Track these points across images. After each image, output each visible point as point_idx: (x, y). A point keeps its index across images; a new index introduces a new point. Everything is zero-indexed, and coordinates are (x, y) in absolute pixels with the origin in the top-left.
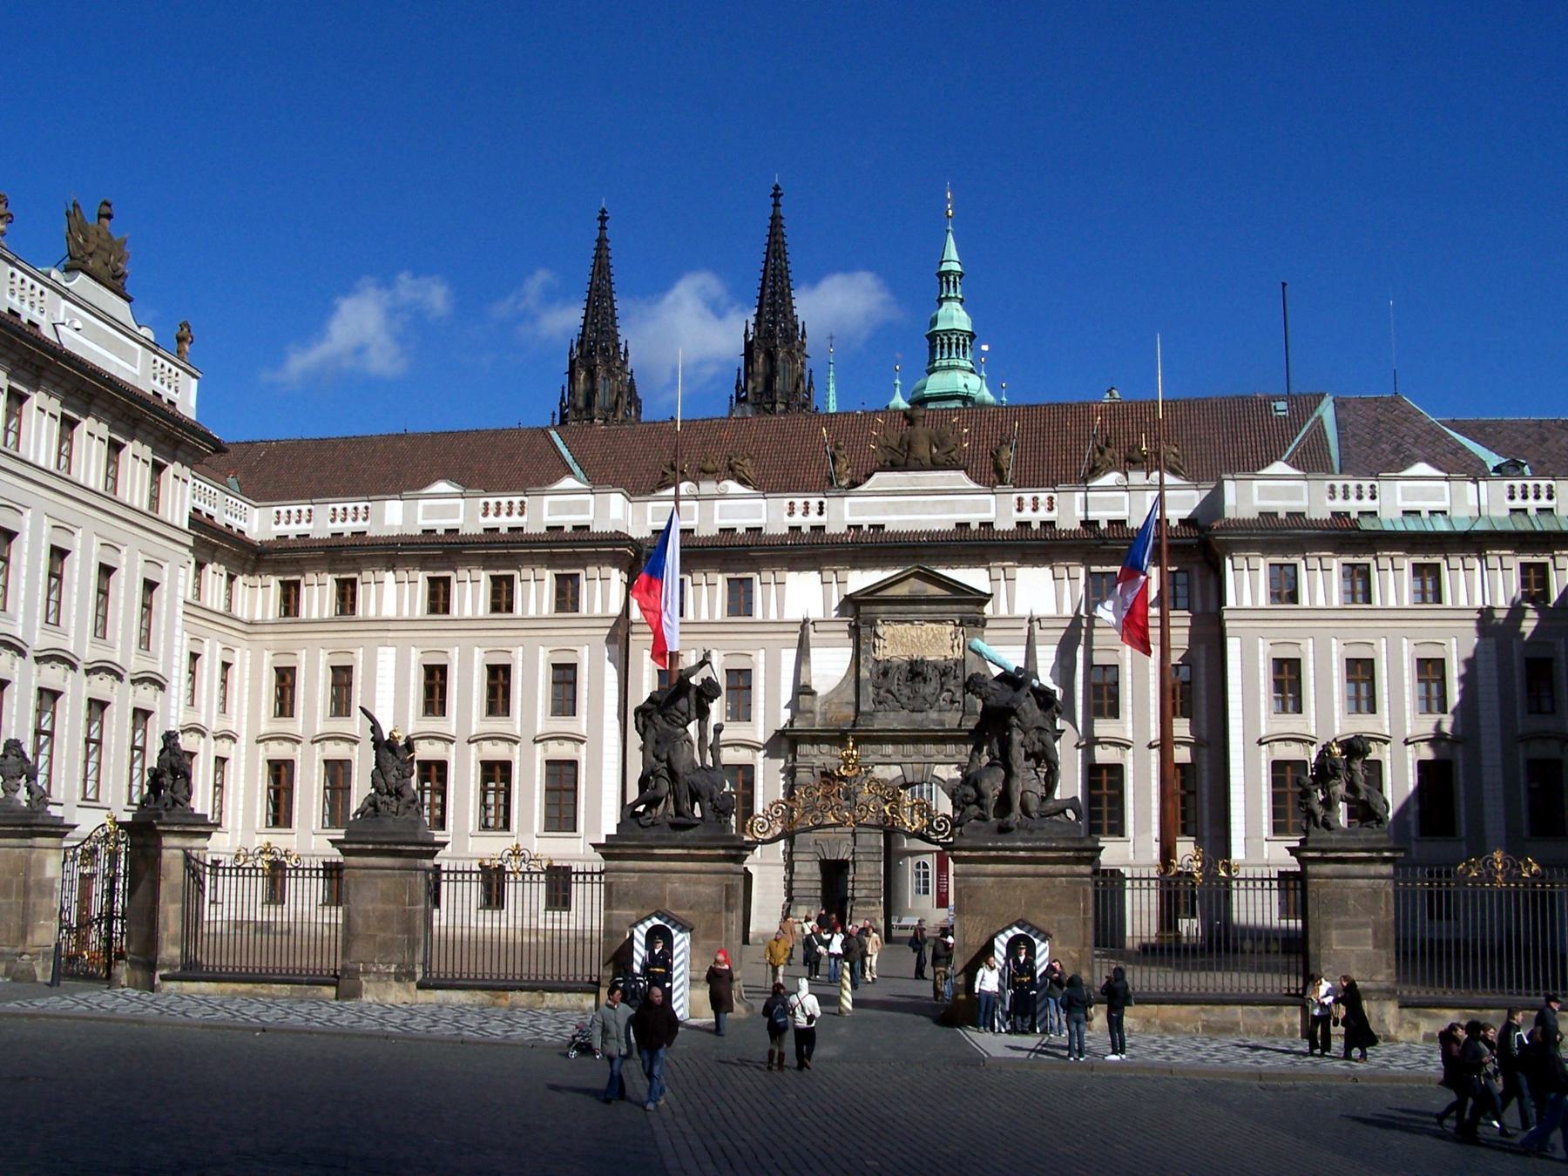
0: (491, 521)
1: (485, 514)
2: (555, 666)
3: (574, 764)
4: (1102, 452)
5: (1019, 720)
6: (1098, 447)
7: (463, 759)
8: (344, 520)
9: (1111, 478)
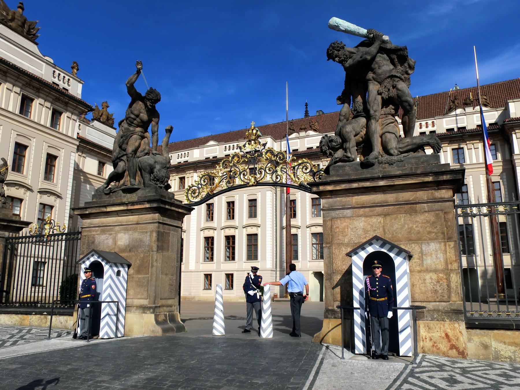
0: (228, 152)
1: (225, 150)
2: (250, 200)
3: (256, 235)
4: (453, 102)
5: (374, 73)
6: (452, 101)
7: (219, 235)
8: (181, 158)
9: (459, 111)
